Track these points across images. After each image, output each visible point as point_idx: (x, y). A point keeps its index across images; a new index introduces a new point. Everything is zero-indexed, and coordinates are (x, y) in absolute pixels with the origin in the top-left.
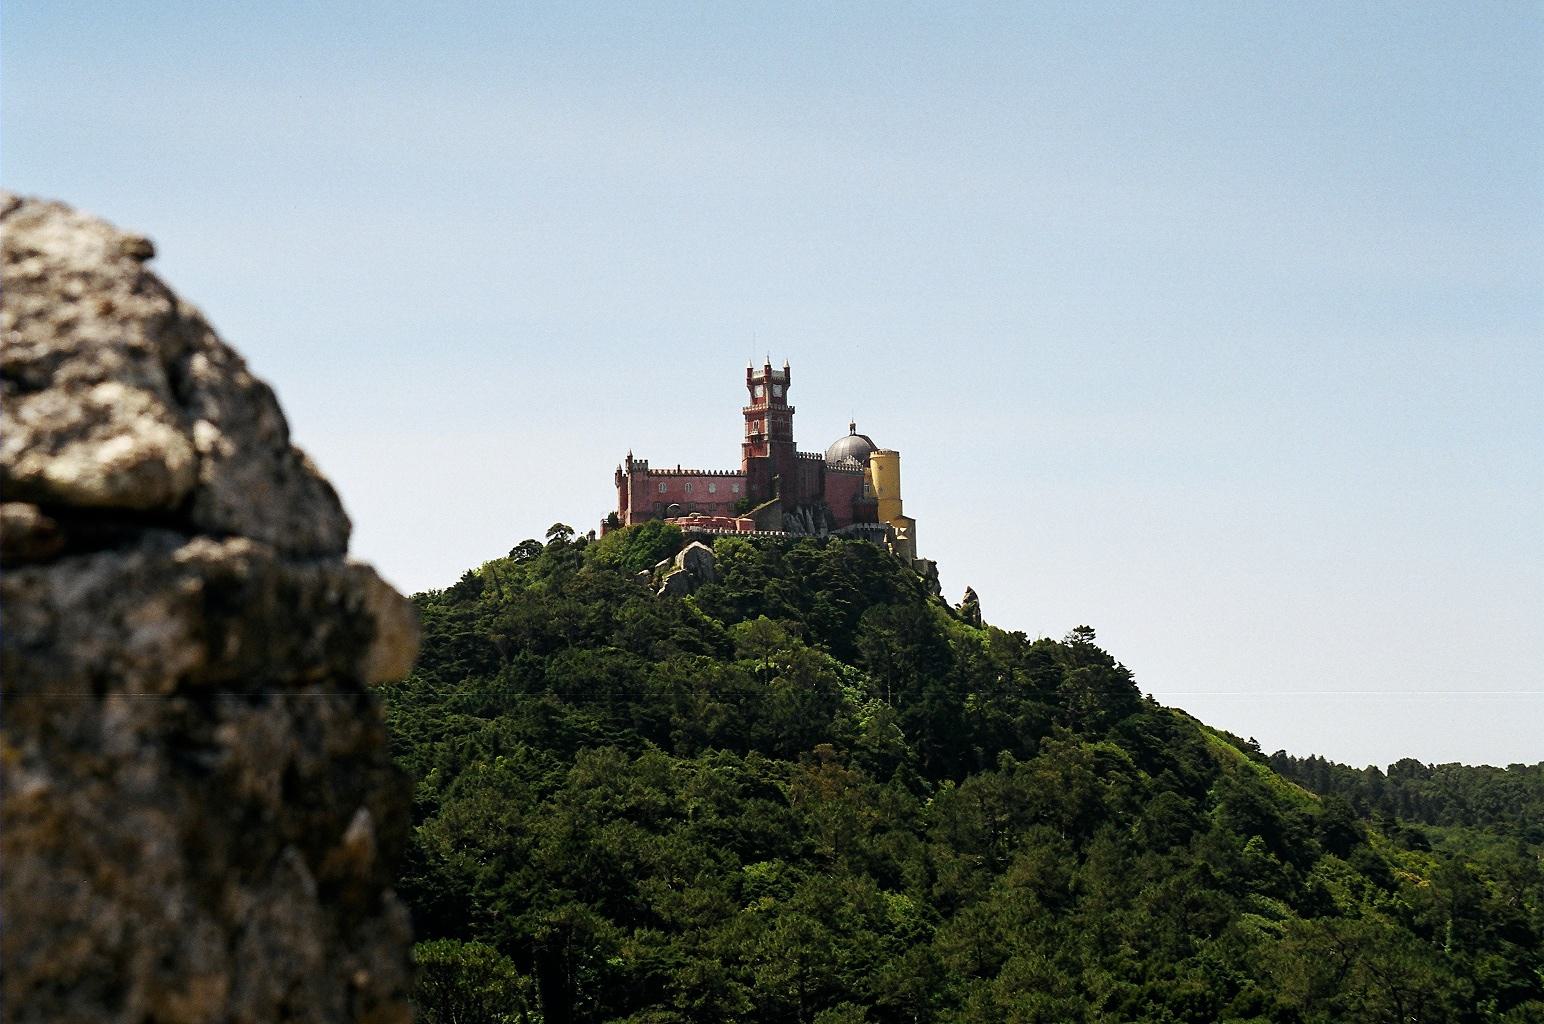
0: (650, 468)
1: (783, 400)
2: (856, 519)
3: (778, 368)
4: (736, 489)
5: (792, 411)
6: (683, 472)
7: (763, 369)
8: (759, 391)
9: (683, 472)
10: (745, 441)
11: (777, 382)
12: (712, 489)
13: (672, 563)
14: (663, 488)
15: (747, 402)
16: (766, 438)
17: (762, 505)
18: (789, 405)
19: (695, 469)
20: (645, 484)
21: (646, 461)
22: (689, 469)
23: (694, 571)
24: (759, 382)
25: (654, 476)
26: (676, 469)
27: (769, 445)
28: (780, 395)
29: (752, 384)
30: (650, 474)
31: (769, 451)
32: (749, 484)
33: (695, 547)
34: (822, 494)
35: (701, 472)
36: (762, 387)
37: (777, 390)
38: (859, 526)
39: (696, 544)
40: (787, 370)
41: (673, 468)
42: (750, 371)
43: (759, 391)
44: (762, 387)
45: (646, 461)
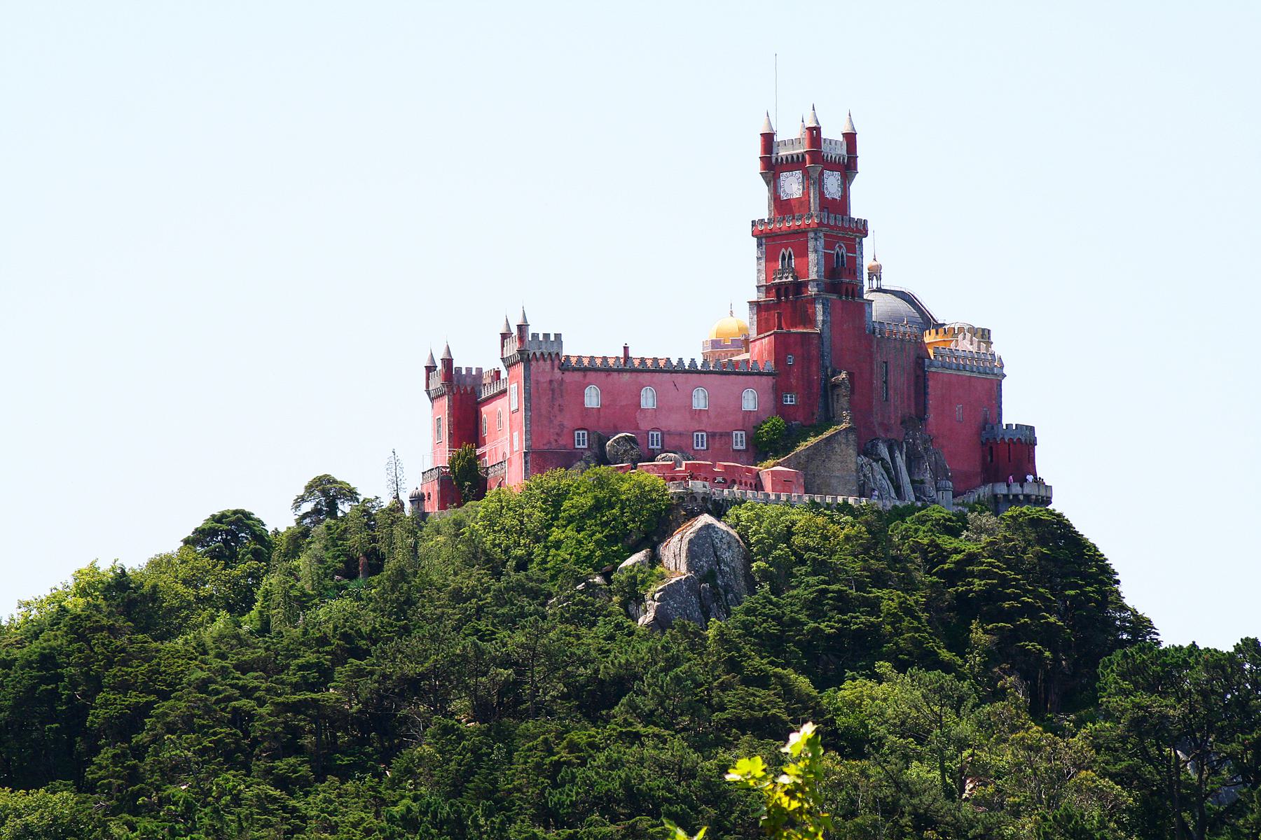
0: (566, 352)
1: (841, 206)
2: (992, 473)
3: (832, 132)
4: (750, 402)
5: (861, 229)
6: (636, 363)
7: (806, 136)
8: (792, 186)
9: (636, 363)
10: (754, 296)
11: (832, 165)
12: (700, 401)
13: (655, 560)
14: (592, 398)
15: (762, 210)
16: (812, 290)
17: (812, 441)
18: (856, 213)
19: (661, 355)
20: (555, 389)
21: (558, 336)
22: (649, 354)
23: (710, 577)
24: (794, 163)
25: (574, 370)
26: (621, 355)
27: (819, 307)
28: (837, 196)
29: (772, 167)
30: (566, 366)
31: (820, 318)
32: (779, 392)
33: (708, 527)
34: (921, 416)
35: (675, 362)
36: (798, 174)
37: (832, 183)
38: (1001, 489)
39: (706, 519)
40: (850, 138)
41: (614, 352)
42: (768, 140)
43: (792, 186)
44: (798, 174)
45: (558, 336)
